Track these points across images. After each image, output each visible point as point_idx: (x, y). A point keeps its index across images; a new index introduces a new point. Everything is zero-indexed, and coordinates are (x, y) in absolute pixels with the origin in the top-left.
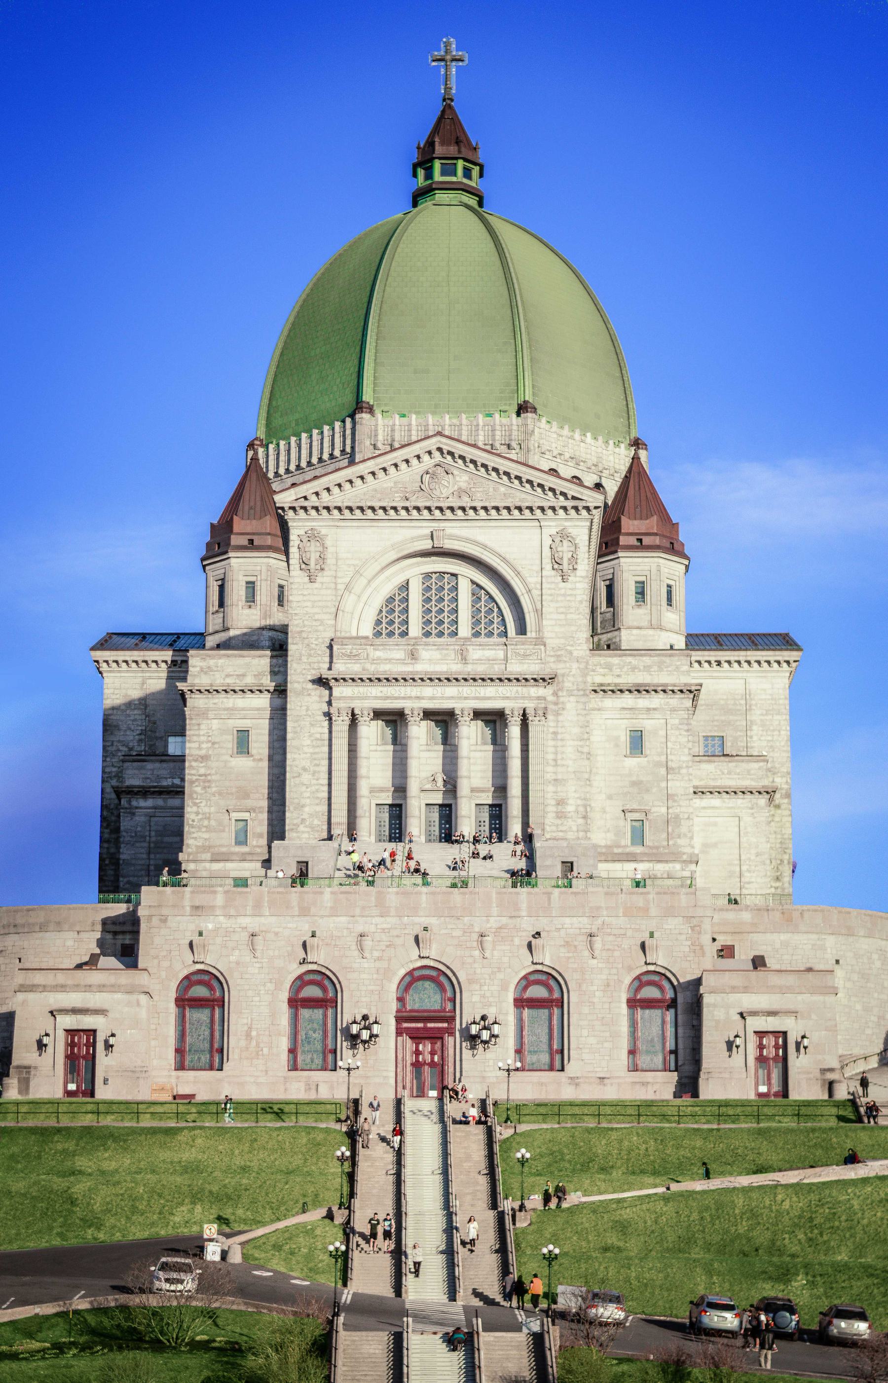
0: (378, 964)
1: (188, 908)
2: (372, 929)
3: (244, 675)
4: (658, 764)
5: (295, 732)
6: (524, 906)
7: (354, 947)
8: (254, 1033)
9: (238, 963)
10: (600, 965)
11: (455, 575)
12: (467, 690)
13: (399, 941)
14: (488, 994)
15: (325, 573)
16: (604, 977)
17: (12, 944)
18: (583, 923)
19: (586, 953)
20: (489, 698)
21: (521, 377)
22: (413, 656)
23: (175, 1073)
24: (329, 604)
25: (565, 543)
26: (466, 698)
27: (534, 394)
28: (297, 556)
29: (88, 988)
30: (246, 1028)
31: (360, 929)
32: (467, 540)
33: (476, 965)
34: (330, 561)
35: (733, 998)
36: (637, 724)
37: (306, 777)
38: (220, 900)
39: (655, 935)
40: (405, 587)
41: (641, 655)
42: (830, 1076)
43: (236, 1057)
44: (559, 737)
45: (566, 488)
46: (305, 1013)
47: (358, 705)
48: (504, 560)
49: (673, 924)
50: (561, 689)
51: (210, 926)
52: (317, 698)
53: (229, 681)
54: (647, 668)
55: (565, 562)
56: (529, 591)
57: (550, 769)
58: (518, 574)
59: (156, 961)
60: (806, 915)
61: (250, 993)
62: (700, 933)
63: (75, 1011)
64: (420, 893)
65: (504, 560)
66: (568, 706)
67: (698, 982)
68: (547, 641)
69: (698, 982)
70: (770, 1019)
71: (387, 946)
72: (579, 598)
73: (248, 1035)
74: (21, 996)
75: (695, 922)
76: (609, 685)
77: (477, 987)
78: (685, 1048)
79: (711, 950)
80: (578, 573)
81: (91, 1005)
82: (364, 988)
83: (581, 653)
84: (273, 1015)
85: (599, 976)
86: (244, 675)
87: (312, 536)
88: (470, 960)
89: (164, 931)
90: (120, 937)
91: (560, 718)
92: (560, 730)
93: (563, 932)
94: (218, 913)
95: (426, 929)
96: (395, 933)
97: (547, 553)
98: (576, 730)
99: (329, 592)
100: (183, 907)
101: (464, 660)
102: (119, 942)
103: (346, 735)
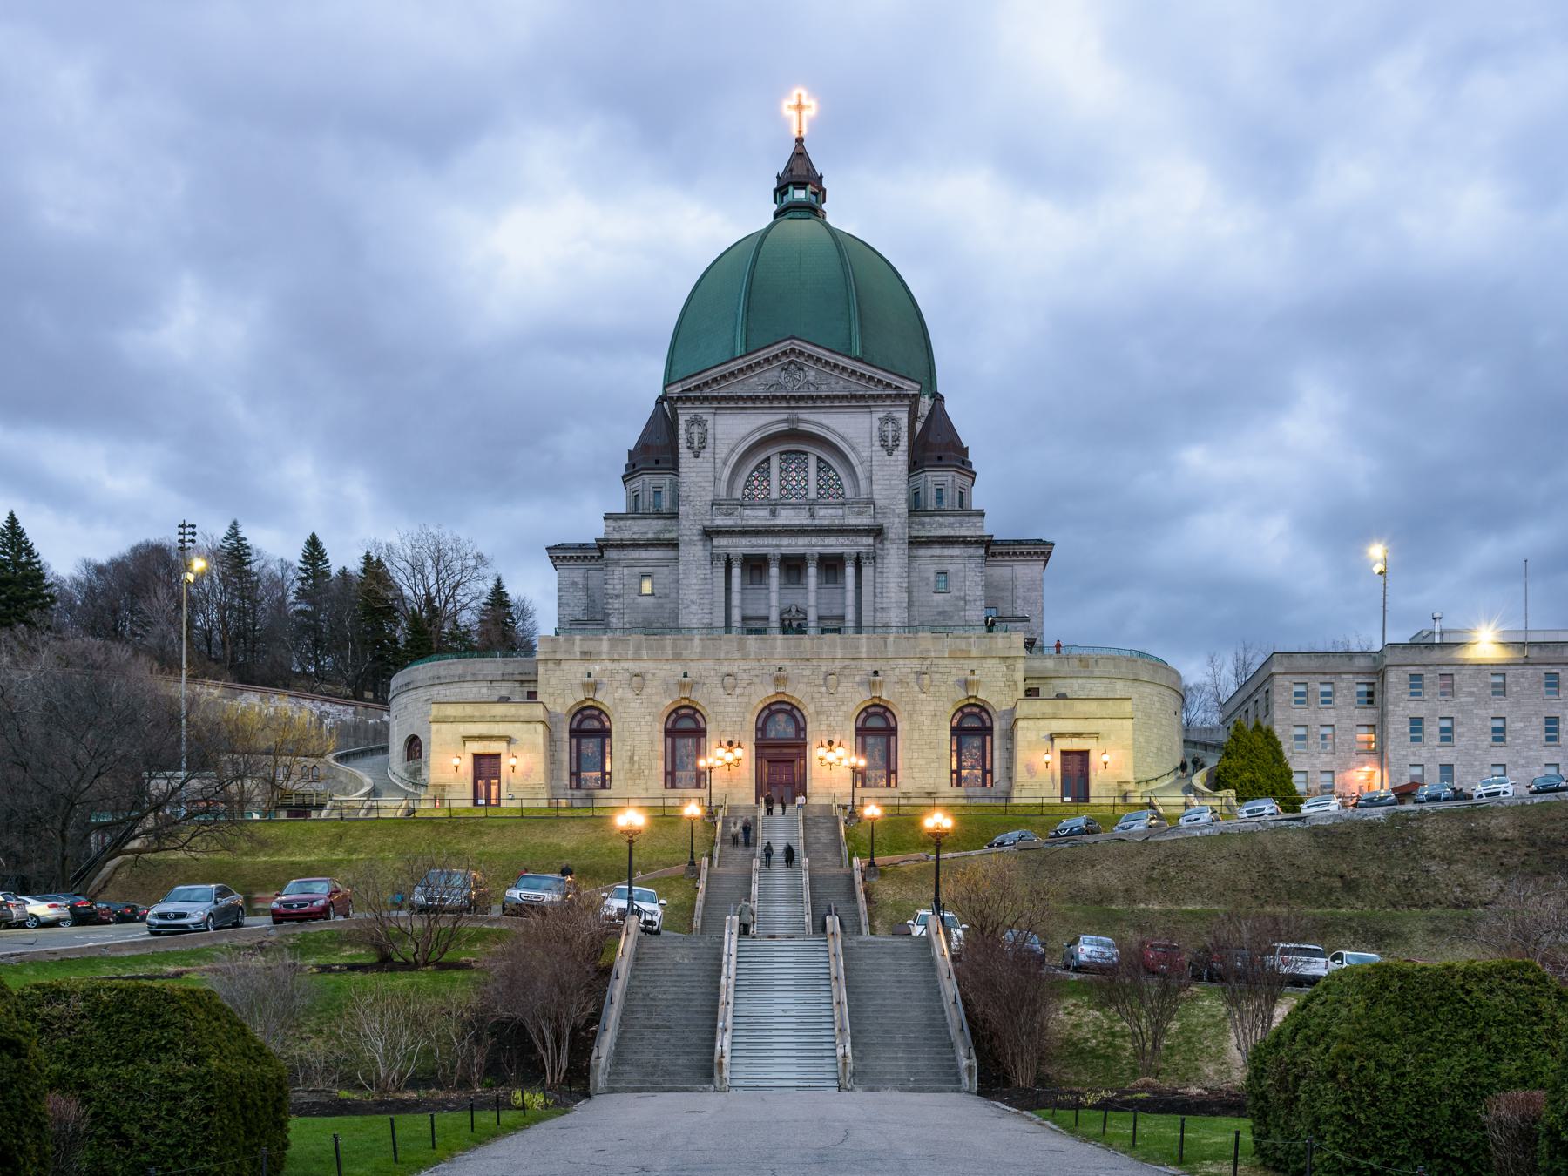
0: (740, 700)
1: (578, 653)
2: (735, 670)
3: (646, 533)
4: (959, 598)
5: (685, 574)
6: (864, 650)
7: (719, 685)
8: (636, 758)
9: (621, 700)
10: (929, 699)
11: (805, 453)
12: (814, 540)
13: (755, 679)
14: (833, 723)
15: (706, 450)
16: (932, 708)
17: (437, 692)
18: (916, 664)
19: (917, 689)
20: (831, 546)
21: (853, 339)
22: (773, 513)
23: (569, 792)
24: (710, 474)
25: (890, 424)
26: (814, 546)
27: (863, 352)
28: (684, 437)
29: (493, 720)
30: (629, 754)
31: (726, 668)
32: (814, 423)
33: (823, 700)
34: (710, 440)
35: (1042, 723)
36: (944, 568)
37: (694, 608)
38: (605, 646)
39: (976, 673)
40: (768, 460)
41: (948, 515)
42: (1126, 787)
43: (622, 777)
44: (885, 575)
45: (890, 379)
46: (680, 742)
47: (731, 551)
48: (843, 438)
49: (989, 664)
50: (886, 539)
51: (598, 668)
52: (701, 548)
53: (634, 537)
54: (951, 525)
55: (890, 439)
56: (861, 463)
57: (878, 600)
58: (853, 449)
59: (552, 698)
60: (1100, 662)
61: (632, 724)
62: (1014, 670)
63: (481, 738)
64: (776, 639)
65: (843, 438)
66: (892, 552)
67: (1014, 709)
68: (876, 502)
69: (1014, 709)
70: (1075, 740)
71: (748, 684)
72: (900, 468)
73: (631, 759)
74: (434, 727)
75: (1009, 661)
76: (922, 537)
77: (824, 718)
78: (1000, 768)
79: (1022, 687)
80: (900, 448)
81: (495, 733)
82: (728, 719)
83: (902, 511)
84: (652, 742)
85: (927, 708)
86: (646, 533)
87: (697, 421)
88: (819, 695)
89: (558, 673)
90: (526, 685)
91: (885, 561)
92: (885, 570)
93: (897, 671)
94: (604, 657)
95: (780, 669)
96: (753, 673)
97: (876, 433)
98: (897, 570)
99: (709, 465)
100: (574, 653)
101: (812, 515)
102: (526, 690)
103: (723, 574)
